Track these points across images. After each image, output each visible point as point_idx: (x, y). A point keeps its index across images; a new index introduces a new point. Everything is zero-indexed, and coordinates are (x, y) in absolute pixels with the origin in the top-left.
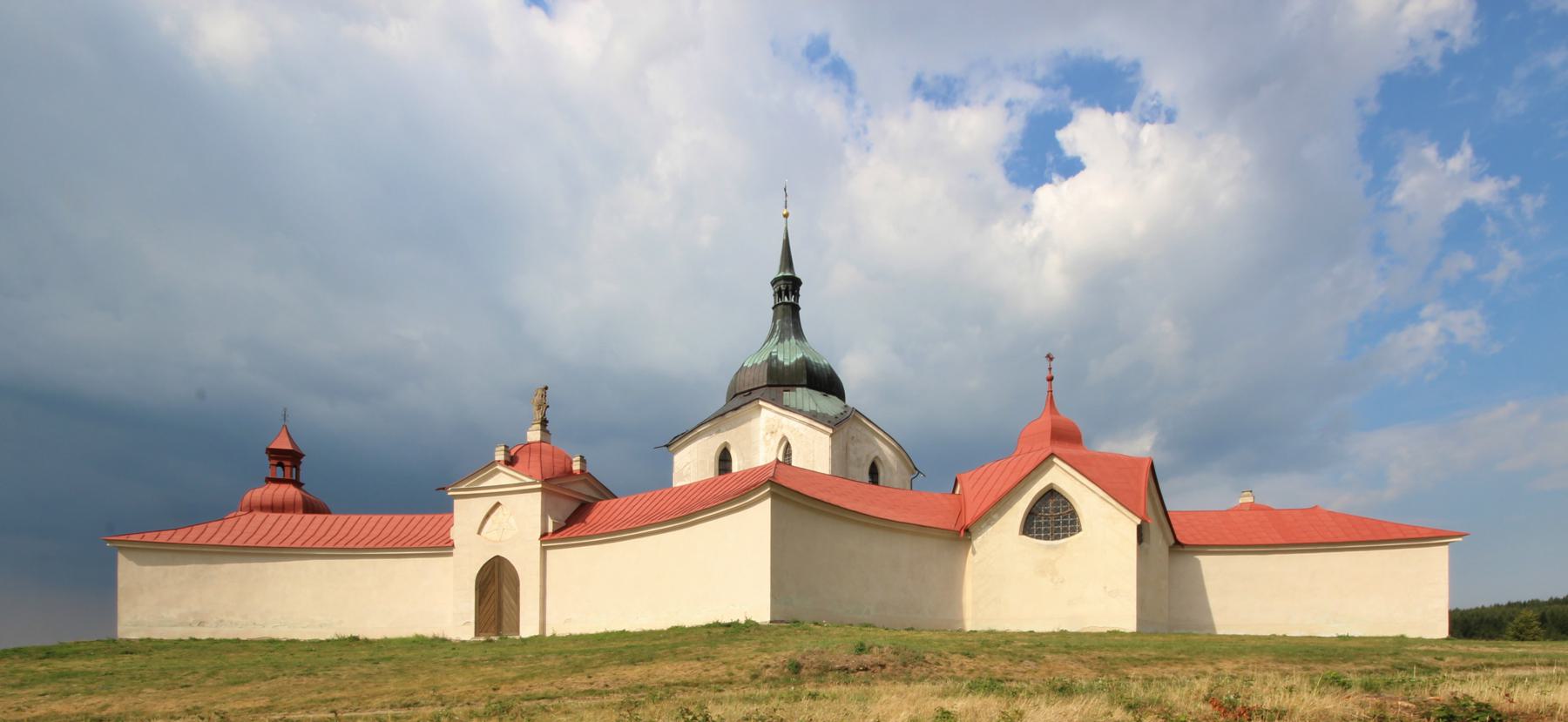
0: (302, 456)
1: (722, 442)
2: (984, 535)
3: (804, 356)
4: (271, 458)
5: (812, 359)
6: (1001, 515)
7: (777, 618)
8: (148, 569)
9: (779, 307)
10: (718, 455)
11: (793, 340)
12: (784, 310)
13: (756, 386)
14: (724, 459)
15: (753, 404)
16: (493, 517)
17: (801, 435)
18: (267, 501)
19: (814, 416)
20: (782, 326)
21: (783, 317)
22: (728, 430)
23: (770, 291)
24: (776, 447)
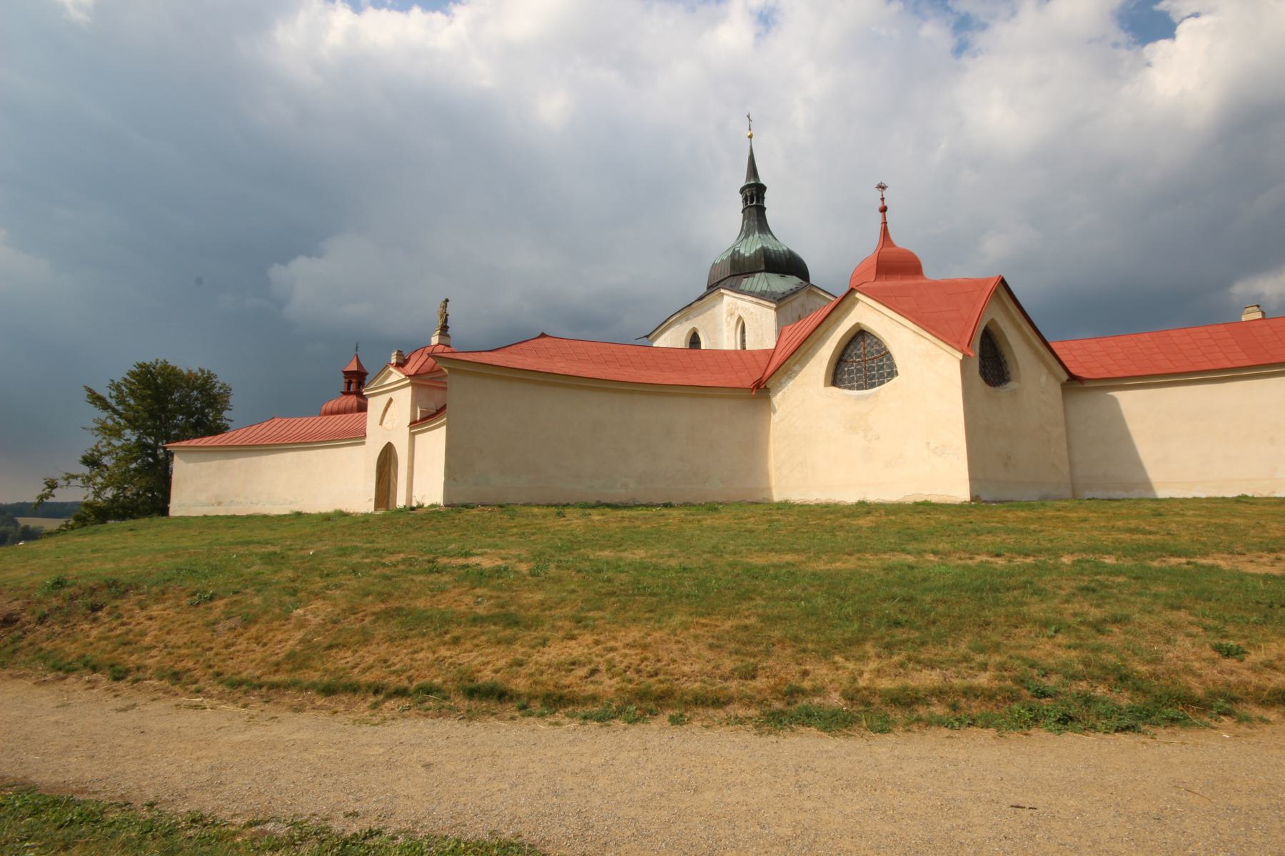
0: (367, 374)
1: (687, 331)
2: (785, 390)
3: (762, 247)
4: (345, 378)
5: (770, 247)
6: (802, 366)
7: (455, 501)
8: (191, 465)
9: (746, 211)
10: (689, 339)
11: (757, 234)
12: (749, 212)
13: (722, 278)
14: (694, 340)
15: (716, 293)
16: (389, 410)
17: (752, 313)
18: (335, 408)
19: (762, 295)
20: (748, 224)
21: (749, 218)
22: (695, 317)
23: (740, 198)
24: (734, 327)
